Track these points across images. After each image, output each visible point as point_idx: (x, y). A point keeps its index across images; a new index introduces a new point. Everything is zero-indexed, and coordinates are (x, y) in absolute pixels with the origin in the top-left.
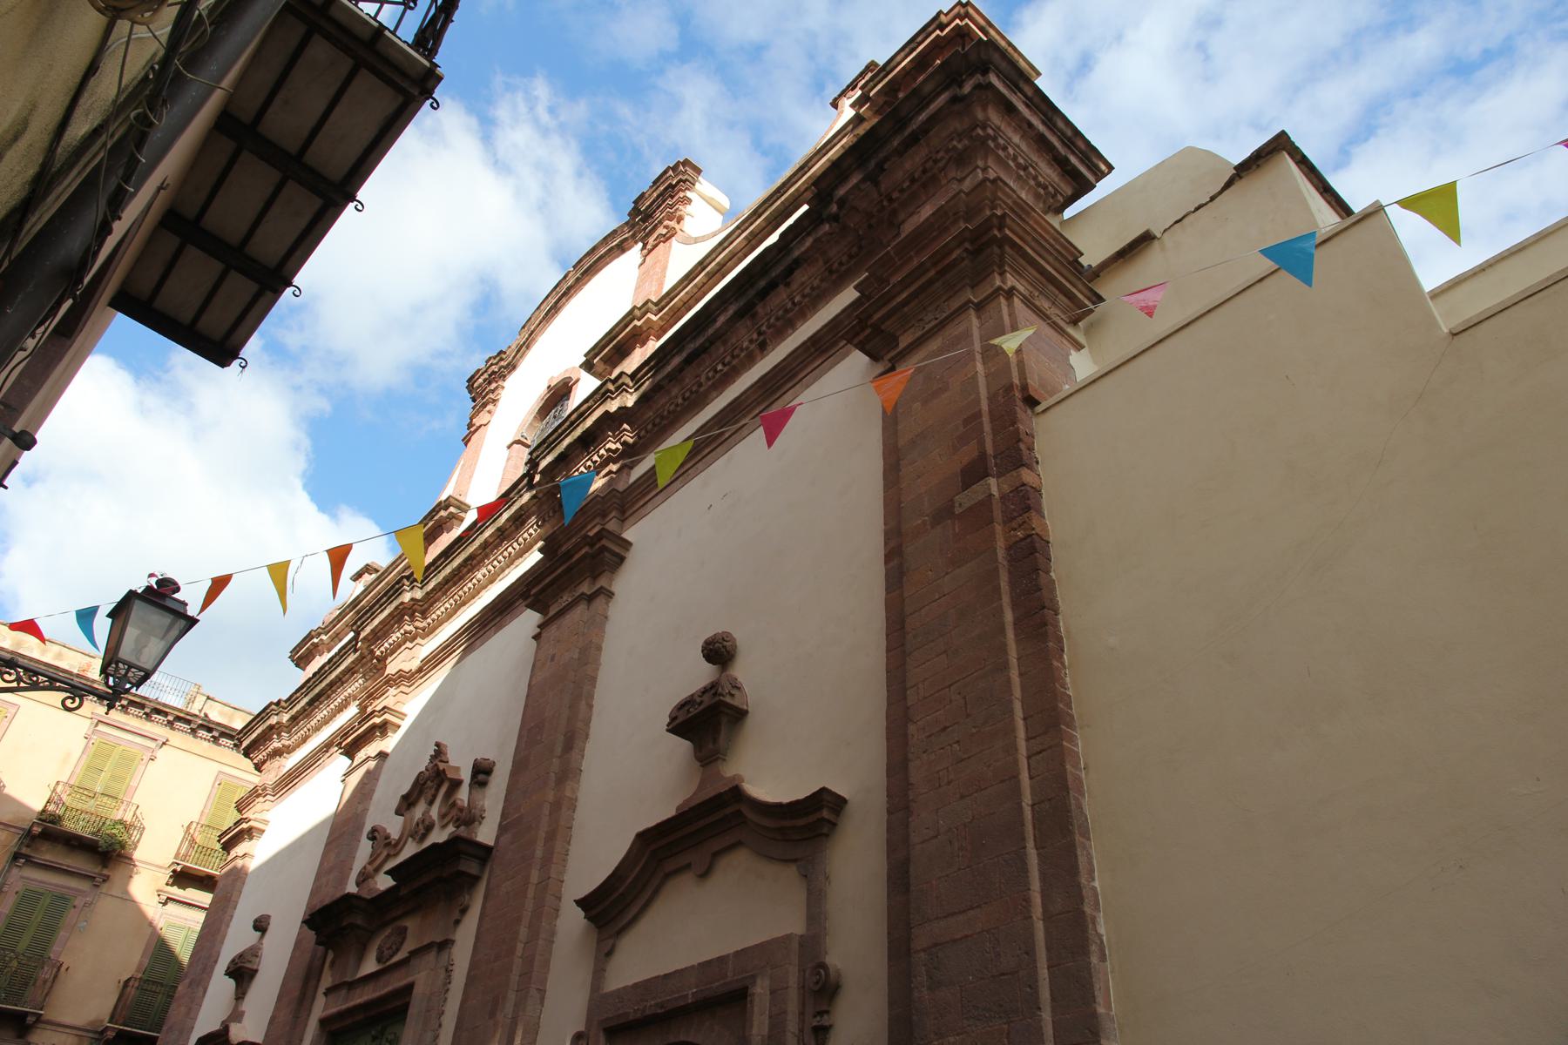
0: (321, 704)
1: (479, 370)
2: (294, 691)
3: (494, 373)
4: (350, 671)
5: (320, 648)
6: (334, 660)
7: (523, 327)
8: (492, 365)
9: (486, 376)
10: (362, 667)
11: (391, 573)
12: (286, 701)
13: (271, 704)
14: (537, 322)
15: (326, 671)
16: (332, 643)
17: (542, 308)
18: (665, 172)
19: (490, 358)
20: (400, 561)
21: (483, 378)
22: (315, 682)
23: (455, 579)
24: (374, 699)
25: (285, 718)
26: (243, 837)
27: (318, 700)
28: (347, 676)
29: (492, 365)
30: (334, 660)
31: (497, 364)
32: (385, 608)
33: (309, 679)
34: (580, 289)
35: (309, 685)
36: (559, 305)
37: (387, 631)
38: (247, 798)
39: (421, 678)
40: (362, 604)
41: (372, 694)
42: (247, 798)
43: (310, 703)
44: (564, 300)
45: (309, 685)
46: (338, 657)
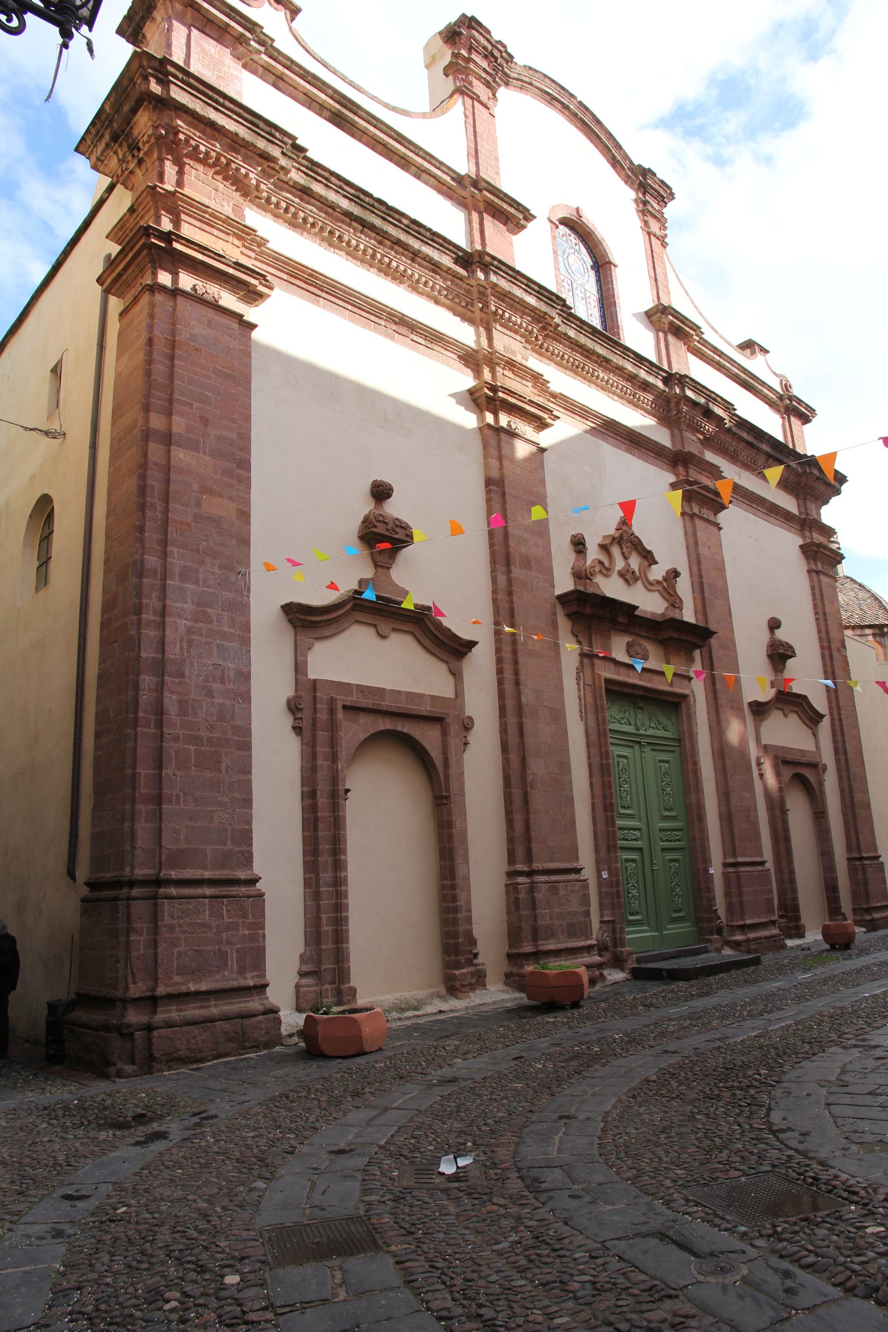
0: (362, 232)
1: (488, 32)
2: (332, 169)
3: (496, 59)
4: (435, 267)
5: (241, 49)
6: (422, 230)
7: (530, 68)
8: (501, 52)
9: (490, 47)
10: (452, 281)
11: (417, 155)
12: (306, 158)
13: (294, 138)
14: (546, 89)
15: (400, 222)
16: (261, 70)
17: (546, 80)
18: (669, 188)
19: (505, 47)
20: (437, 164)
21: (486, 43)
22: (373, 206)
23: (585, 353)
24: (510, 369)
25: (296, 176)
26: (240, 289)
27: (364, 226)
28: (426, 264)
29: (501, 52)
30: (422, 230)
31: (502, 57)
32: (530, 294)
33: (370, 196)
34: (571, 121)
35: (362, 196)
36: (555, 103)
37: (518, 310)
38: (212, 215)
39: (549, 400)
40: (356, 119)
41: (514, 366)
42: (212, 215)
43: (347, 214)
44: (559, 106)
45: (362, 196)
46: (428, 234)
